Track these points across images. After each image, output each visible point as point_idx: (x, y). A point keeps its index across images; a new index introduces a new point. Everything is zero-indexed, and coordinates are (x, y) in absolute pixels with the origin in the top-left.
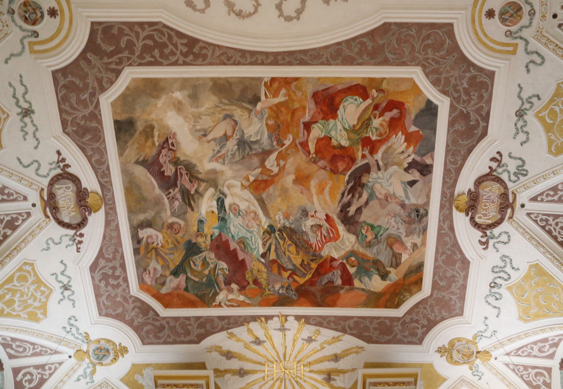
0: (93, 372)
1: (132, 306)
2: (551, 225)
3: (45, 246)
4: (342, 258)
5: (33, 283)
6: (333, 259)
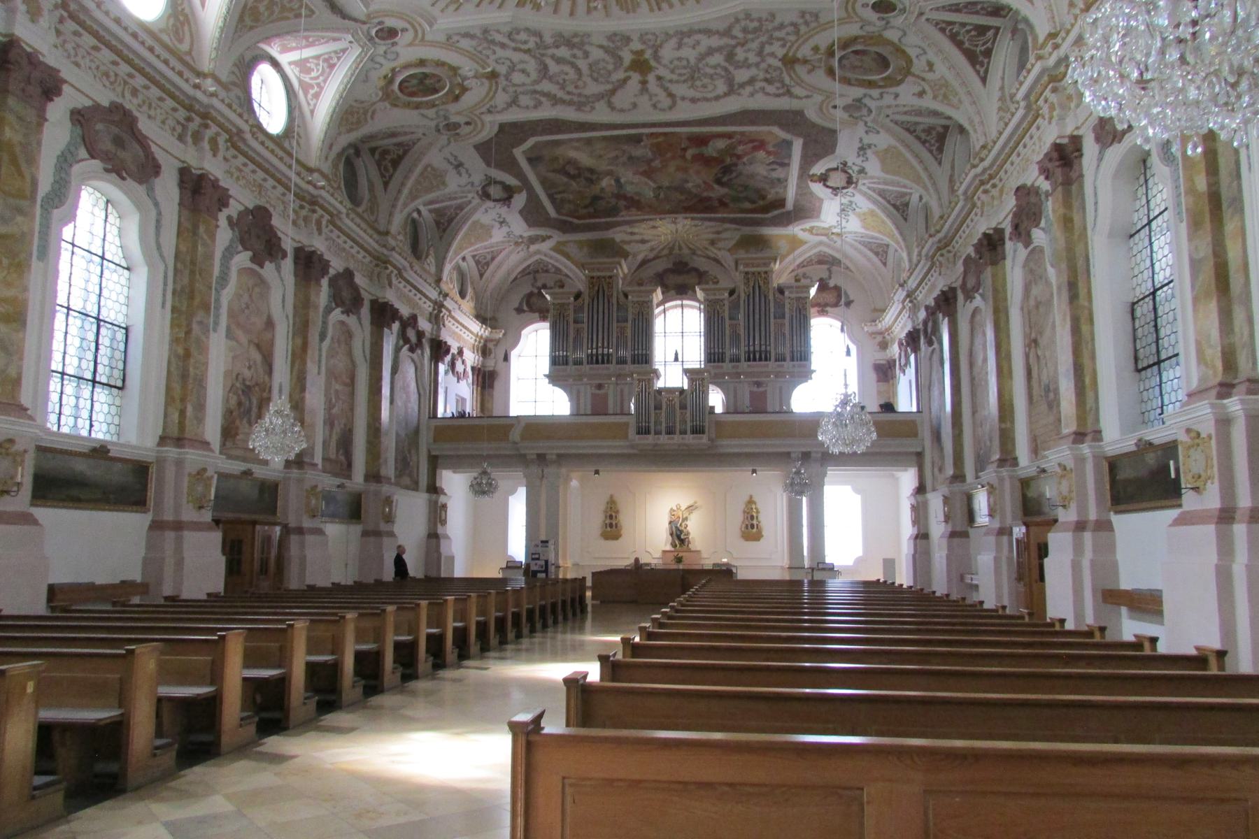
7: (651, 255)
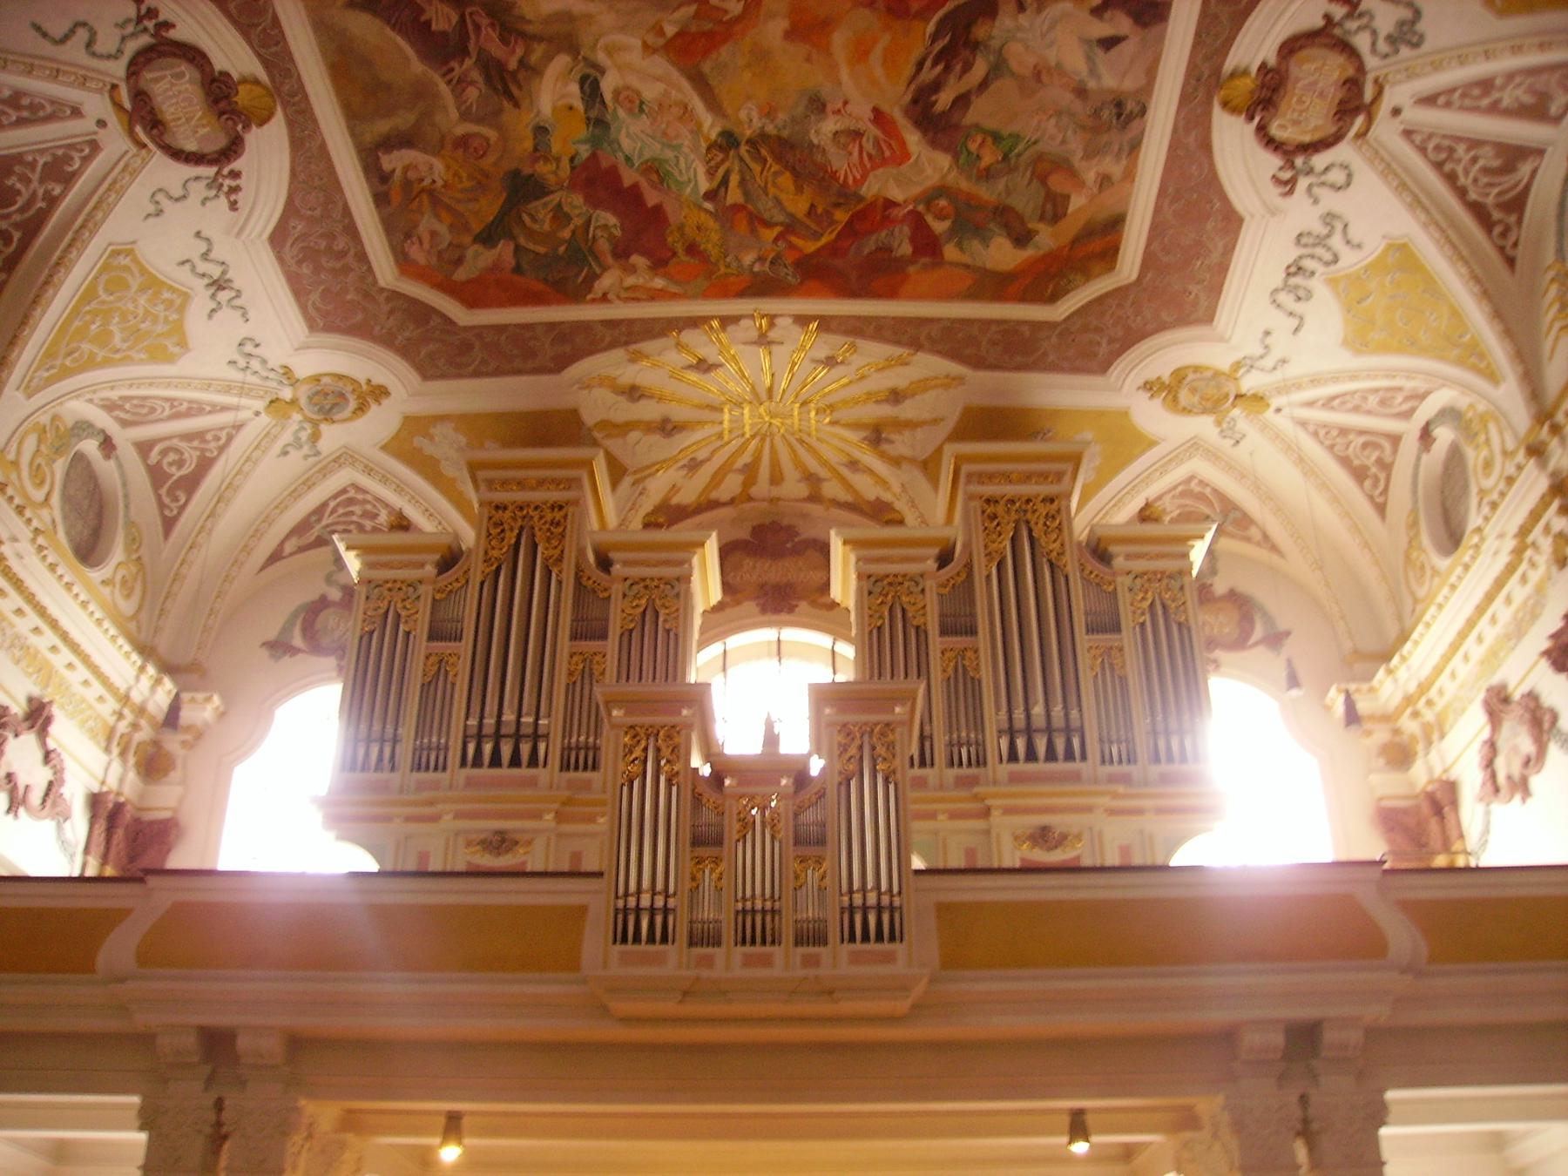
0: (315, 437)
1: (386, 308)
2: (1459, 161)
3: (152, 209)
4: (916, 200)
5: (142, 290)
6: (890, 204)
7: (688, 495)
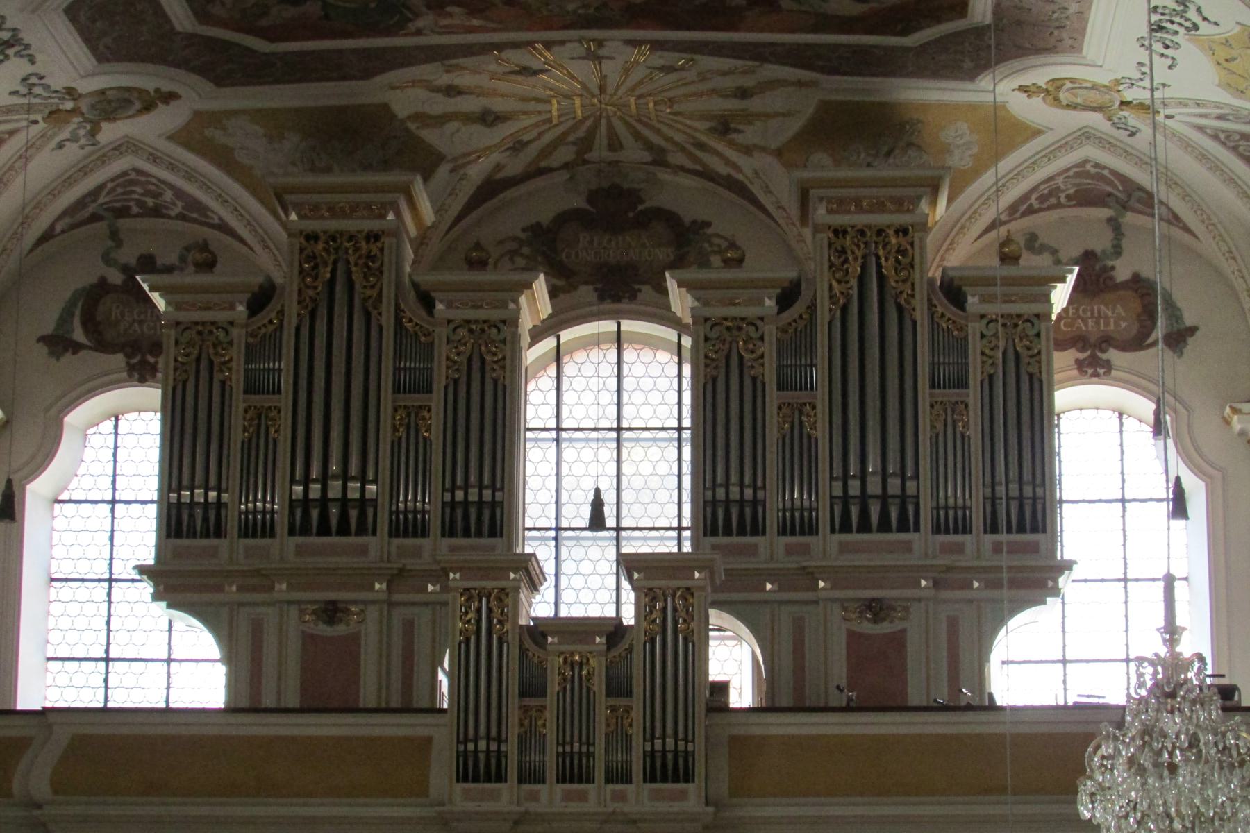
0: (93, 133)
7: (515, 166)
